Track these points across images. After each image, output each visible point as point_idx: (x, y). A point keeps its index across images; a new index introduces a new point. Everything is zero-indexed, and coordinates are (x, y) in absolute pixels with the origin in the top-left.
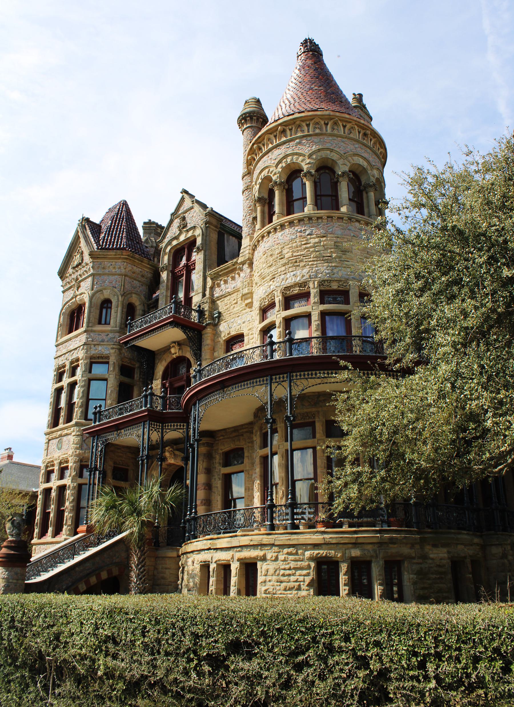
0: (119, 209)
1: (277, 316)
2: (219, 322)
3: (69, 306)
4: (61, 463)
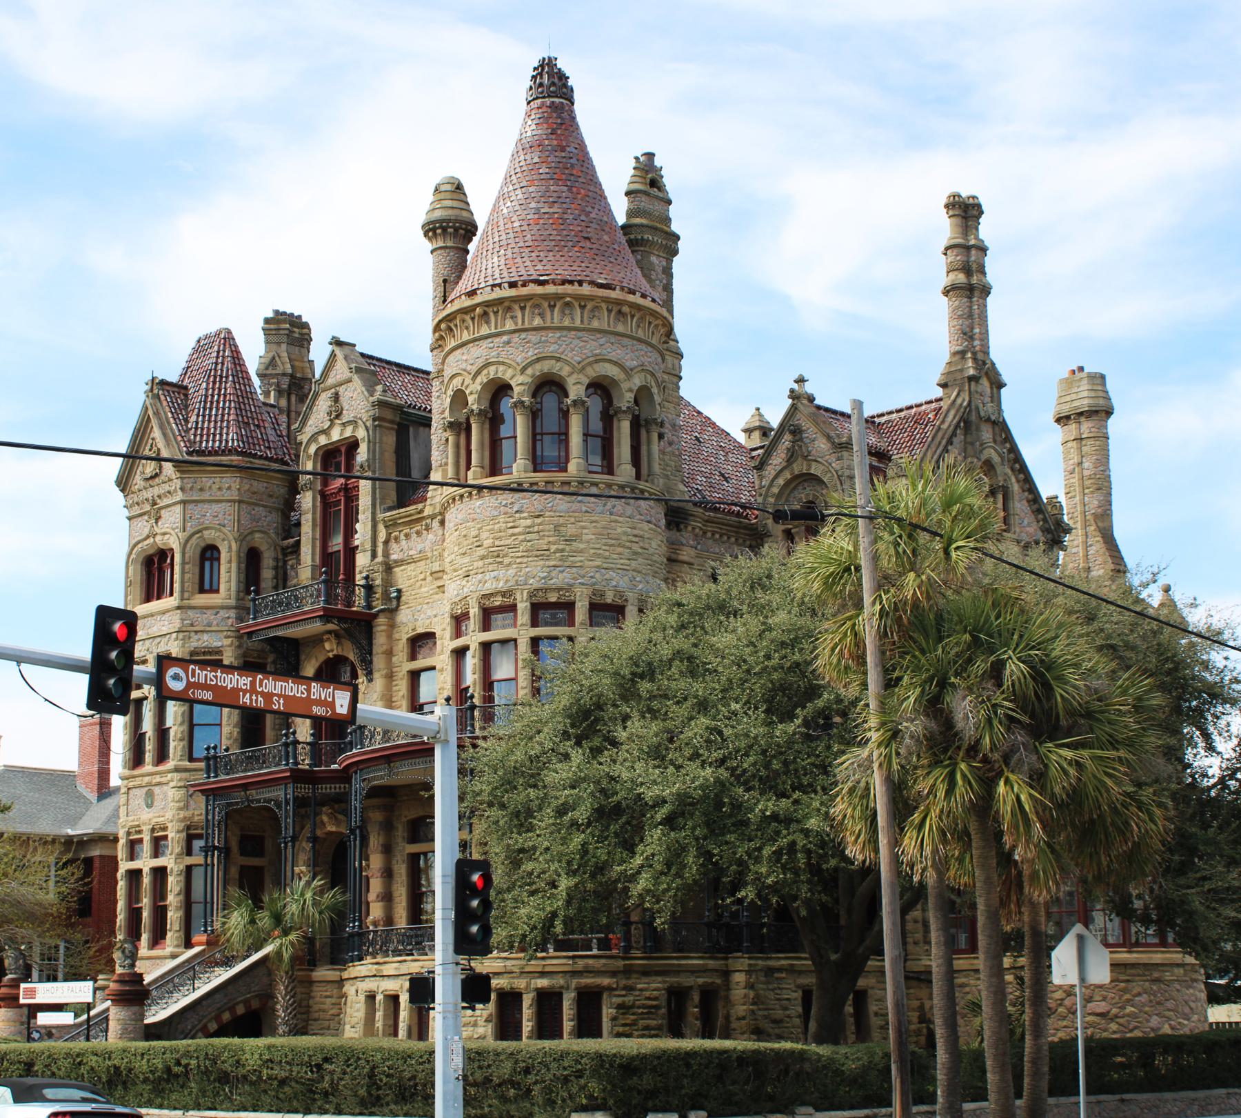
1: (474, 638)
2: (398, 605)
4: (153, 830)
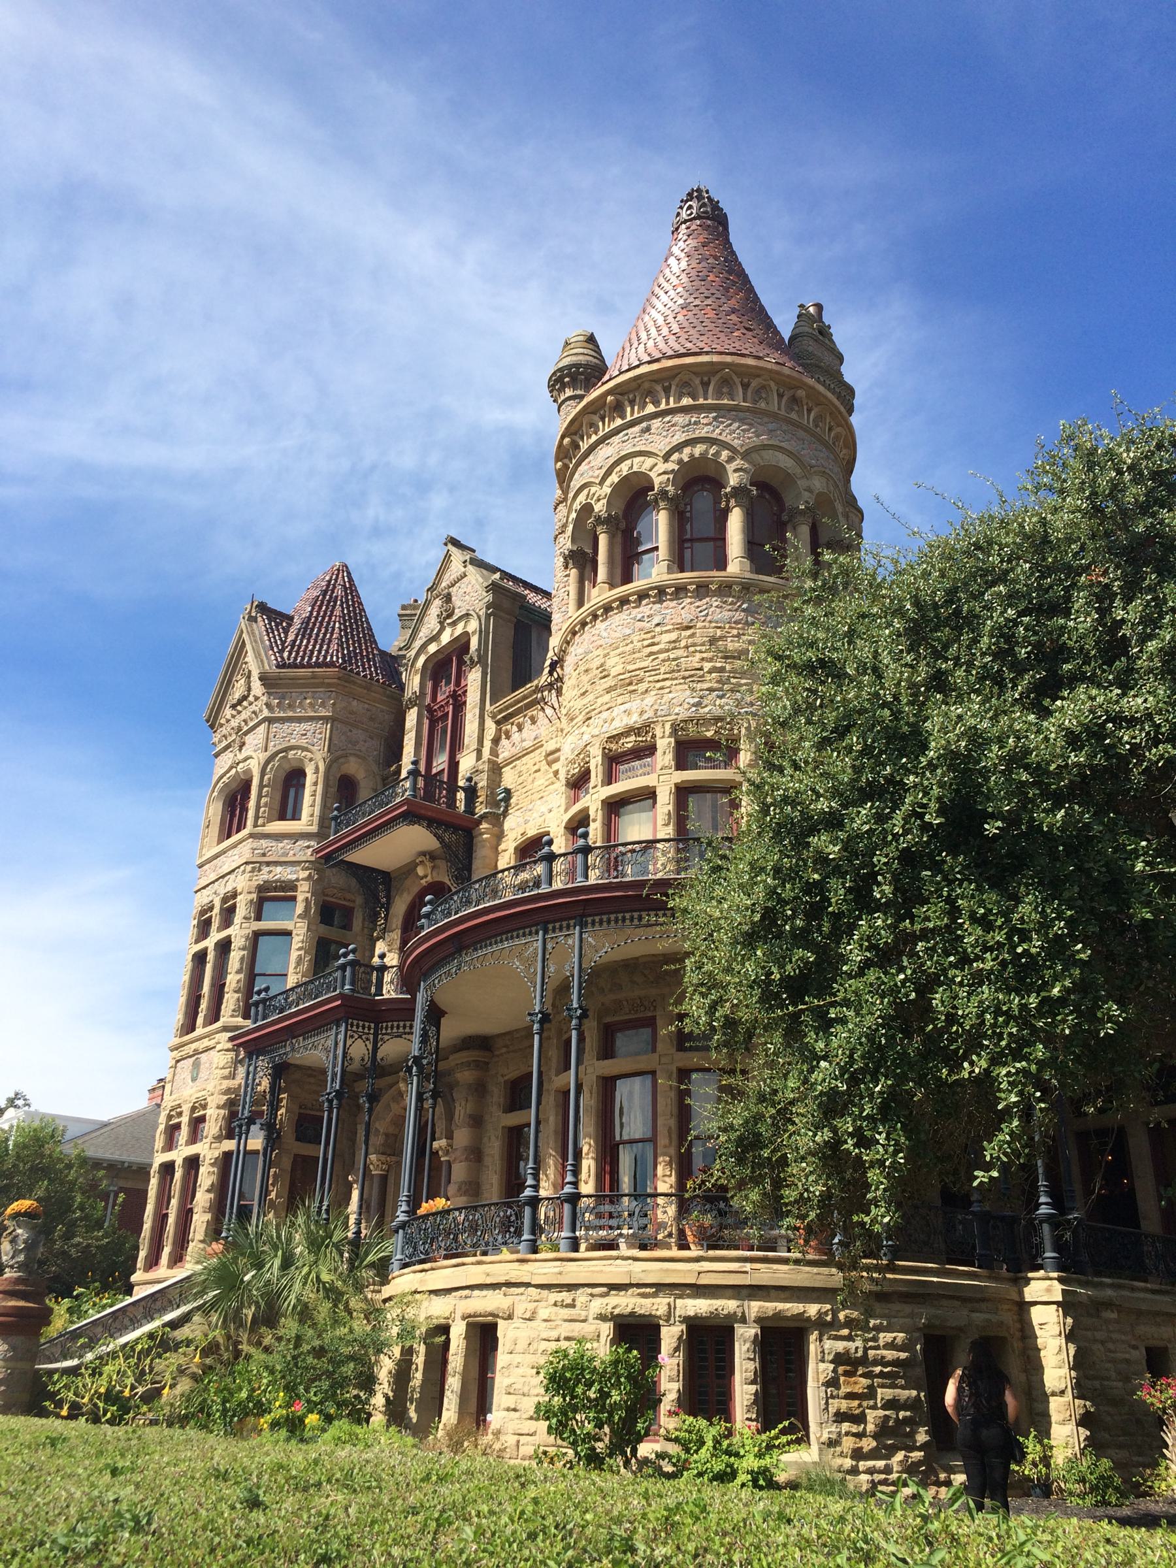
0: (329, 582)
1: (594, 799)
2: (507, 808)
3: (226, 785)
4: (193, 1109)
